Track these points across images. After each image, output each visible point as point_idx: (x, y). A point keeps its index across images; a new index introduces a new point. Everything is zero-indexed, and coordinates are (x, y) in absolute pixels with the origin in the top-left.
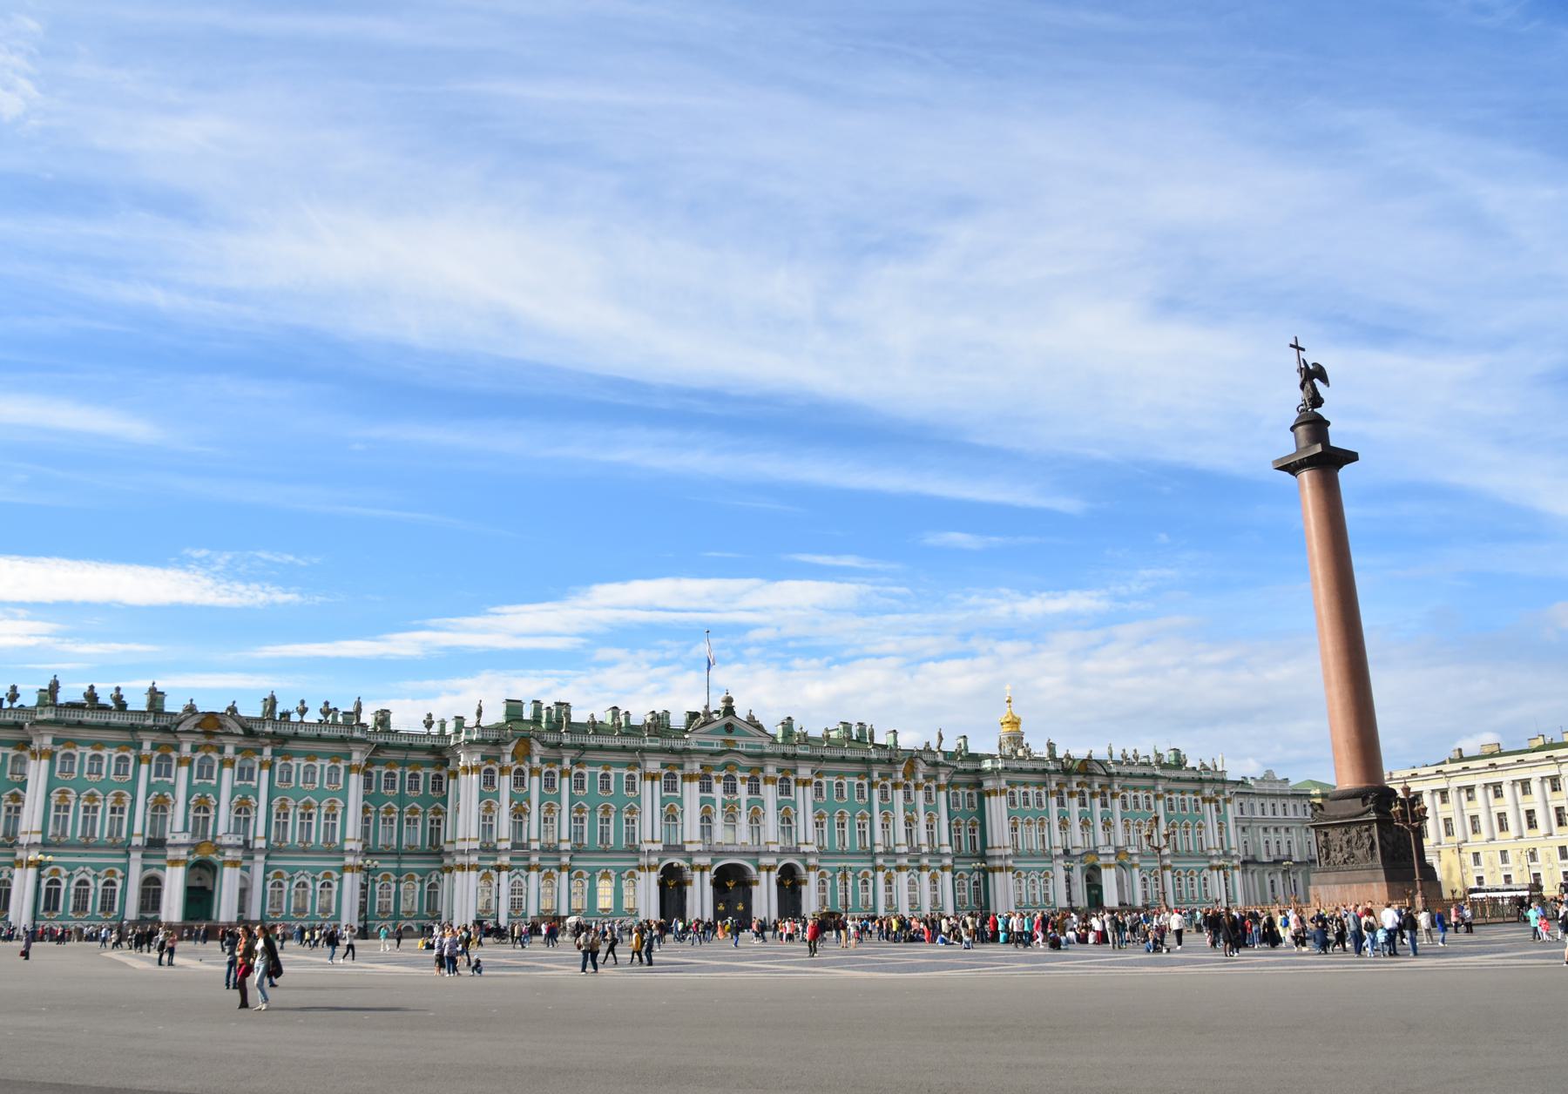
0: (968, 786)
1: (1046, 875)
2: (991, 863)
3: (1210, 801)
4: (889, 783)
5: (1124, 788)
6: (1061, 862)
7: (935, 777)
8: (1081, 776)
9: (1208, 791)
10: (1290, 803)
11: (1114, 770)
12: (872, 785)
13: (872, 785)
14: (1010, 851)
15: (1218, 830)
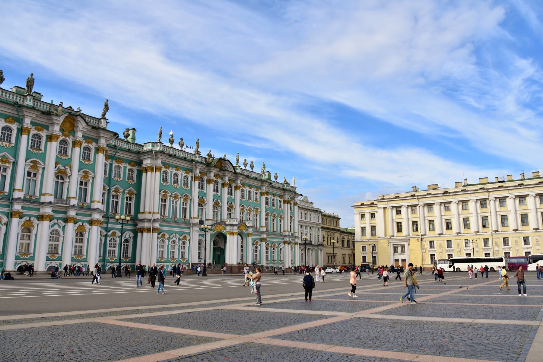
0: (130, 162)
1: (184, 238)
2: (140, 225)
3: (288, 202)
4: (44, 134)
5: (243, 185)
6: (197, 229)
7: (97, 141)
8: (219, 169)
9: (287, 197)
10: (314, 215)
11: (238, 171)
12: (21, 131)
13: (21, 131)
14: (158, 216)
15: (290, 221)
